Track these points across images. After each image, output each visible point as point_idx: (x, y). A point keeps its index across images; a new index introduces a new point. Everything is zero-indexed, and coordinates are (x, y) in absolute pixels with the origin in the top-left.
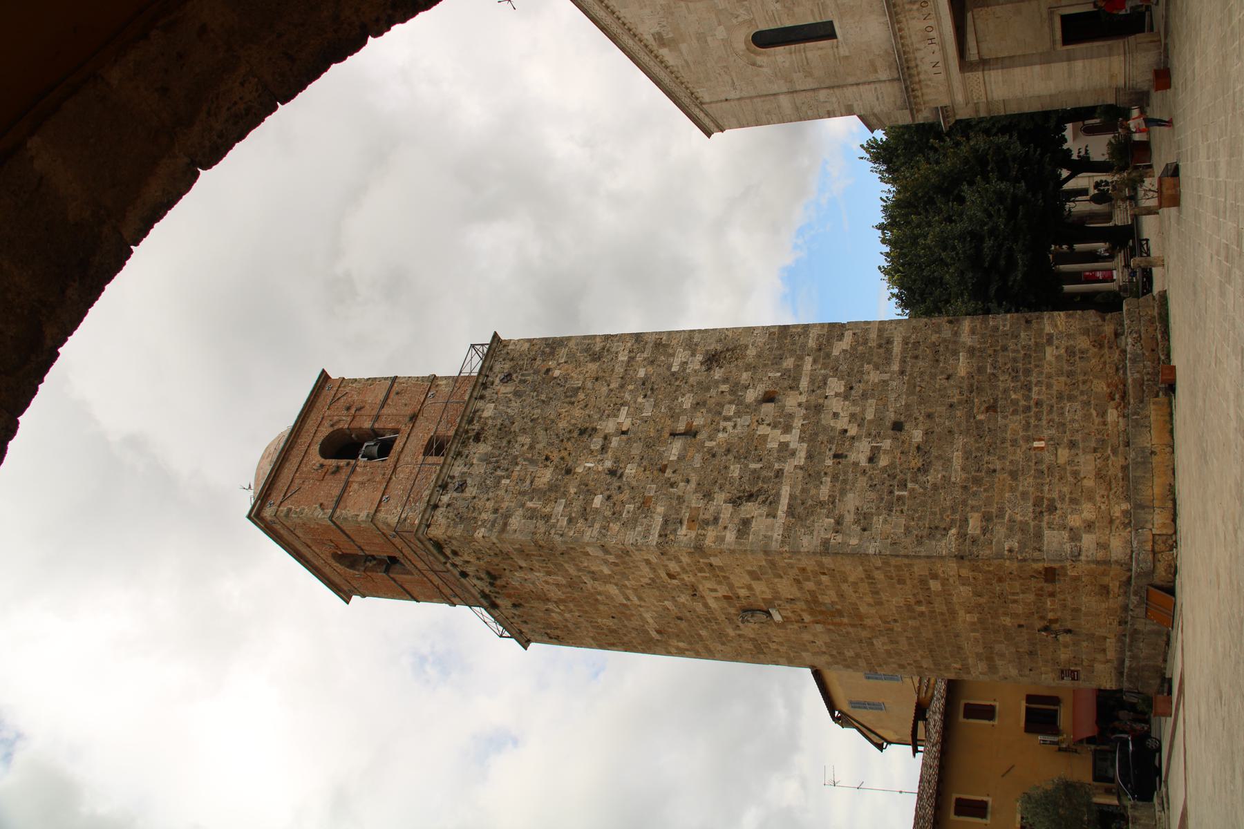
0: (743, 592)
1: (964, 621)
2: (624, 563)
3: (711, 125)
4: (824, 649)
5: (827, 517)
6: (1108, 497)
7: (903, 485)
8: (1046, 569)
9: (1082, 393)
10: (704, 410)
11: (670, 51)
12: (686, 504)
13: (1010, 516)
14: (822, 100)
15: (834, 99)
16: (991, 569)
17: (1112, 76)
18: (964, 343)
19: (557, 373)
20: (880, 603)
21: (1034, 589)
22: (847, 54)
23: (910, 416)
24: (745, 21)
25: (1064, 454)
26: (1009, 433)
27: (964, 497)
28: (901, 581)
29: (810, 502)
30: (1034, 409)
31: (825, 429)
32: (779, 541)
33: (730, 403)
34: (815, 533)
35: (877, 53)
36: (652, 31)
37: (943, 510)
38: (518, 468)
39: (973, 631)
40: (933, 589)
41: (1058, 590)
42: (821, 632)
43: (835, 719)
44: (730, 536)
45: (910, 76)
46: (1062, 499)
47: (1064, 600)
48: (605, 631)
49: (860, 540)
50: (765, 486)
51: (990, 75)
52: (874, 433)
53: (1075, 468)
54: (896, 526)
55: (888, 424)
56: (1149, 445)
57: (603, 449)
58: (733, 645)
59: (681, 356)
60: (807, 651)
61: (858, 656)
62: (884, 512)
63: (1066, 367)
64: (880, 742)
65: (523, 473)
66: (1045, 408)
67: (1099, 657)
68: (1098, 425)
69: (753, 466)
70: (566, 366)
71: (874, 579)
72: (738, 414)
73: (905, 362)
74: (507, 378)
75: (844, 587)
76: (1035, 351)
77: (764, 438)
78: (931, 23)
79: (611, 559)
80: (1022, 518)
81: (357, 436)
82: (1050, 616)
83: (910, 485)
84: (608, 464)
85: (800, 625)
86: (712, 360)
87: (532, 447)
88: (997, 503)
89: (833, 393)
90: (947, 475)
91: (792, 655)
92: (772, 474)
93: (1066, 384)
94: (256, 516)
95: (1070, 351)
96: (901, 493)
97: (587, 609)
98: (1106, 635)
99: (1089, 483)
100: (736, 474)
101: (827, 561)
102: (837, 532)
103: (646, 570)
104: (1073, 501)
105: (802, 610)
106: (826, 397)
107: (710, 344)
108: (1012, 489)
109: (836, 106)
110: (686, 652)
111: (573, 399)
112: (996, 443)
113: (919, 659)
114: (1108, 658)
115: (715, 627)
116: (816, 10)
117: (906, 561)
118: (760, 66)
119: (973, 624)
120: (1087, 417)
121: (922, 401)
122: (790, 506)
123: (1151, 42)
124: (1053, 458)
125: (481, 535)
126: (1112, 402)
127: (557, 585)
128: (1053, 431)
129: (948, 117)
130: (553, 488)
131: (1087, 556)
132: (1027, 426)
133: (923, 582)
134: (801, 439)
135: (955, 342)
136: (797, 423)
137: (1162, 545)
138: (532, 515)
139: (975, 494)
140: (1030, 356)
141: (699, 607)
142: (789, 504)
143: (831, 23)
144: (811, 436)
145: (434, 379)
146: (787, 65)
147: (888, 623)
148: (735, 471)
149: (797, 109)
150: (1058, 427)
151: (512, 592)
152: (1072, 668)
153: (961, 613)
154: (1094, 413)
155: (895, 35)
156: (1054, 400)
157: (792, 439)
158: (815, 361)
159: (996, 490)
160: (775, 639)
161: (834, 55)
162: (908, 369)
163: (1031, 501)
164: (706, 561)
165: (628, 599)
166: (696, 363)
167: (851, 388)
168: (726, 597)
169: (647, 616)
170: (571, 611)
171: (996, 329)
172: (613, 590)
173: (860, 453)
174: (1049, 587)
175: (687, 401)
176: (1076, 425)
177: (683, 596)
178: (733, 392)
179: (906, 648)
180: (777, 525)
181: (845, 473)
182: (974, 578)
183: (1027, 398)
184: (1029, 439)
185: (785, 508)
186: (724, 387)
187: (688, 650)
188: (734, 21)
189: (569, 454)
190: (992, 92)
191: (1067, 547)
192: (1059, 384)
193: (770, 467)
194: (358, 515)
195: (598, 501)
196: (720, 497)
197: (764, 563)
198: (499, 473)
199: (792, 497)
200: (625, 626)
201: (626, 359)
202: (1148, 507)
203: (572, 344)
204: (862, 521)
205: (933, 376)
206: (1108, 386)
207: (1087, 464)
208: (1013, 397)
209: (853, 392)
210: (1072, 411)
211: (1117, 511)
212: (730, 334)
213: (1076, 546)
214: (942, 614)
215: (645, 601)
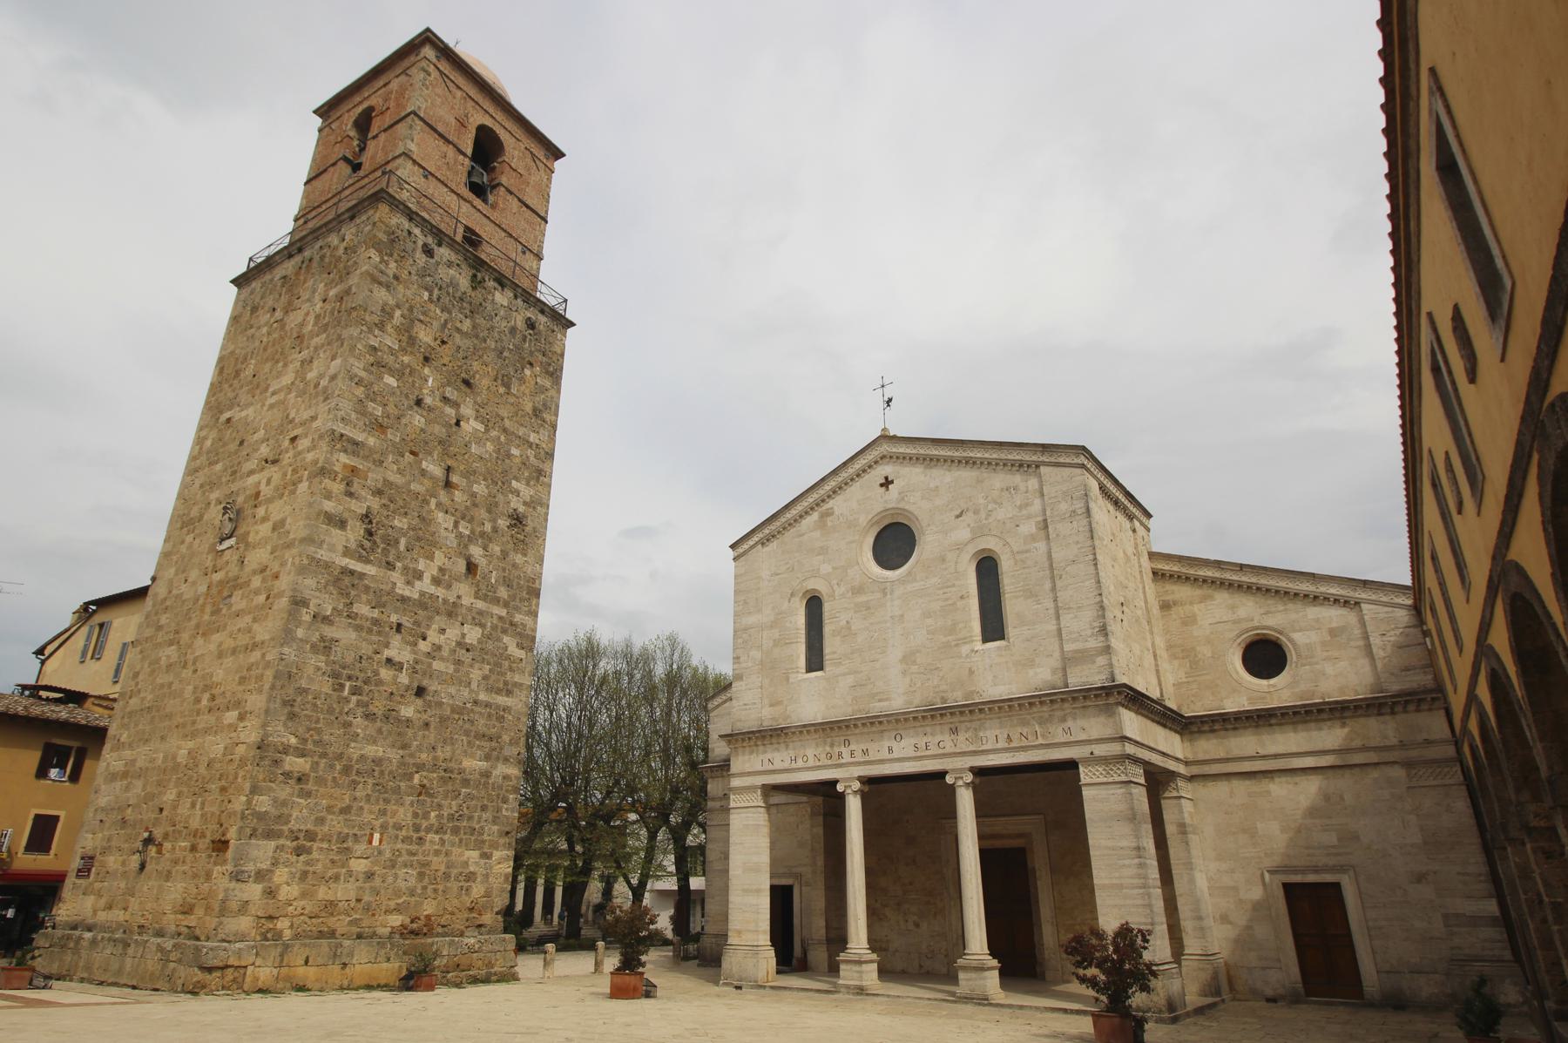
0: (261, 512)
1: (179, 748)
2: (317, 395)
3: (740, 550)
4: (175, 592)
5: (334, 609)
6: (302, 914)
7: (356, 691)
8: (227, 842)
9: (425, 888)
10: (468, 503)
12: (373, 467)
13: (299, 804)
14: (751, 653)
15: (750, 664)
16: (239, 780)
17: (739, 932)
18: (497, 767)
19: (527, 372)
20: (220, 655)
23: (430, 707)
24: (834, 591)
25: (359, 866)
26: (394, 807)
27: (331, 756)
28: (242, 680)
29: (353, 593)
30: (415, 835)
31: (430, 618)
32: (315, 555)
33: (473, 532)
34: (318, 594)
36: (836, 508)
37: (319, 731)
38: (438, 311)
39: (165, 758)
40: (227, 714)
41: (198, 855)
42: (196, 591)
43: (87, 604)
44: (329, 506)
45: (764, 737)
46: (307, 863)
47: (184, 862)
48: (239, 366)
49: (301, 640)
50: (379, 551)
52: (418, 667)
53: (342, 878)
54: (311, 680)
55: (425, 683)
56: (354, 961)
57: (445, 398)
58: (199, 496)
59: (527, 492)
60: (176, 574)
61: (159, 628)
62: (329, 668)
63: (454, 872)
64: (47, 652)
65: (432, 314)
66: (414, 848)
67: (102, 902)
68: (387, 905)
69: (403, 542)
70: (533, 383)
71: (251, 651)
72: (460, 536)
73: (486, 706)
74: (531, 325)
75: (248, 619)
76: (476, 840)
77: (431, 557)
79: (324, 383)
80: (294, 817)
81: (495, 168)
82: (167, 845)
83: (354, 698)
84: (428, 400)
85: (210, 569)
86: (517, 520)
87: (458, 330)
88: (317, 791)
89: (465, 632)
90: (359, 738)
91: (175, 558)
92: (391, 559)
93: (436, 871)
94: (427, 38)
95: (470, 877)
96: (347, 688)
97: (269, 351)
98: (130, 910)
99: (323, 893)
100: (396, 523)
101: (284, 602)
102: (314, 616)
103: (306, 415)
104: (304, 874)
105: (227, 573)
106: (463, 624)
107: (532, 521)
108: (329, 809)
109: (744, 665)
110: (198, 447)
111: (500, 382)
112: (386, 792)
113: (142, 695)
114: (99, 913)
115: (224, 479)
116: (835, 656)
117: (267, 687)
119: (174, 758)
120: (398, 893)
121: (443, 720)
122: (352, 572)
123: (768, 973)
124: (358, 854)
125: (373, 256)
126: (409, 920)
127: (302, 325)
128: (388, 855)
129: (712, 771)
130: (412, 340)
131: (234, 890)
132: (398, 827)
134: (422, 594)
135: (498, 759)
136: (440, 592)
137: (232, 977)
138: (387, 312)
139: (332, 767)
140: (472, 835)
141: (252, 464)
142: (355, 571)
143: (821, 668)
144: (425, 603)
145: (539, 257)
146: (788, 625)
147: (194, 663)
148: (400, 522)
150: (391, 860)
151: (302, 278)
152: (94, 869)
153: (191, 744)
154: (400, 901)
155: (804, 726)
156: (420, 857)
157: (425, 585)
158: (501, 618)
159: (333, 790)
160: (197, 541)
162: (477, 709)
163: (312, 828)
164: (305, 478)
165: (274, 393)
166: (516, 504)
167: (468, 650)
168: (258, 494)
169: (250, 411)
170: (269, 334)
171: (505, 801)
172: (287, 380)
173: (397, 650)
174: (203, 844)
175: (480, 488)
176: (390, 879)
177: (268, 450)
178: (483, 534)
179: (159, 681)
180: (334, 556)
181: (379, 633)
183: (428, 830)
184: (384, 827)
185: (351, 567)
186: (488, 527)
187: (201, 448)
188: (835, 582)
189: (445, 365)
191: (250, 867)
192: (438, 863)
193: (398, 558)
194: (412, 140)
195: (391, 381)
196: (375, 503)
197: (292, 536)
198: (436, 292)
199: (362, 576)
200: (242, 387)
201: (531, 440)
202: (282, 961)
203: (552, 393)
204: (322, 644)
205: (467, 733)
206: (428, 917)
207: (343, 892)
208: (433, 814)
209: (464, 651)
210: (407, 877)
211: (283, 924)
212: (540, 541)
213: (249, 877)
214: (194, 723)
215: (268, 410)
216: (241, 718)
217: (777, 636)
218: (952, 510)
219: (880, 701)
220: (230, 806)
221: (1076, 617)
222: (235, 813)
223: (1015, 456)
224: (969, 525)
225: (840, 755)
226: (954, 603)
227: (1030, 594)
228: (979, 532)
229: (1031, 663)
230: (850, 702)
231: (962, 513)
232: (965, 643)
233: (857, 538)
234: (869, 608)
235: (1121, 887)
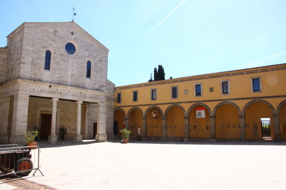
11: (53, 31)
15: (28, 61)
22: (41, 70)
24: (56, 52)
35: (40, 77)
36: (59, 31)
51: (27, 102)
78: (46, 92)
109: (26, 61)
118: (42, 48)
146: (41, 55)
161: (41, 67)
188: (56, 50)
190: (21, 101)
217: (37, 56)
218: (85, 48)
219: (65, 82)
221: (103, 79)
224: (88, 53)
225: (55, 92)
226: (83, 68)
228: (90, 55)
229: (95, 84)
230: (57, 80)
231: (87, 50)
232: (84, 76)
233: (63, 42)
234: (64, 60)
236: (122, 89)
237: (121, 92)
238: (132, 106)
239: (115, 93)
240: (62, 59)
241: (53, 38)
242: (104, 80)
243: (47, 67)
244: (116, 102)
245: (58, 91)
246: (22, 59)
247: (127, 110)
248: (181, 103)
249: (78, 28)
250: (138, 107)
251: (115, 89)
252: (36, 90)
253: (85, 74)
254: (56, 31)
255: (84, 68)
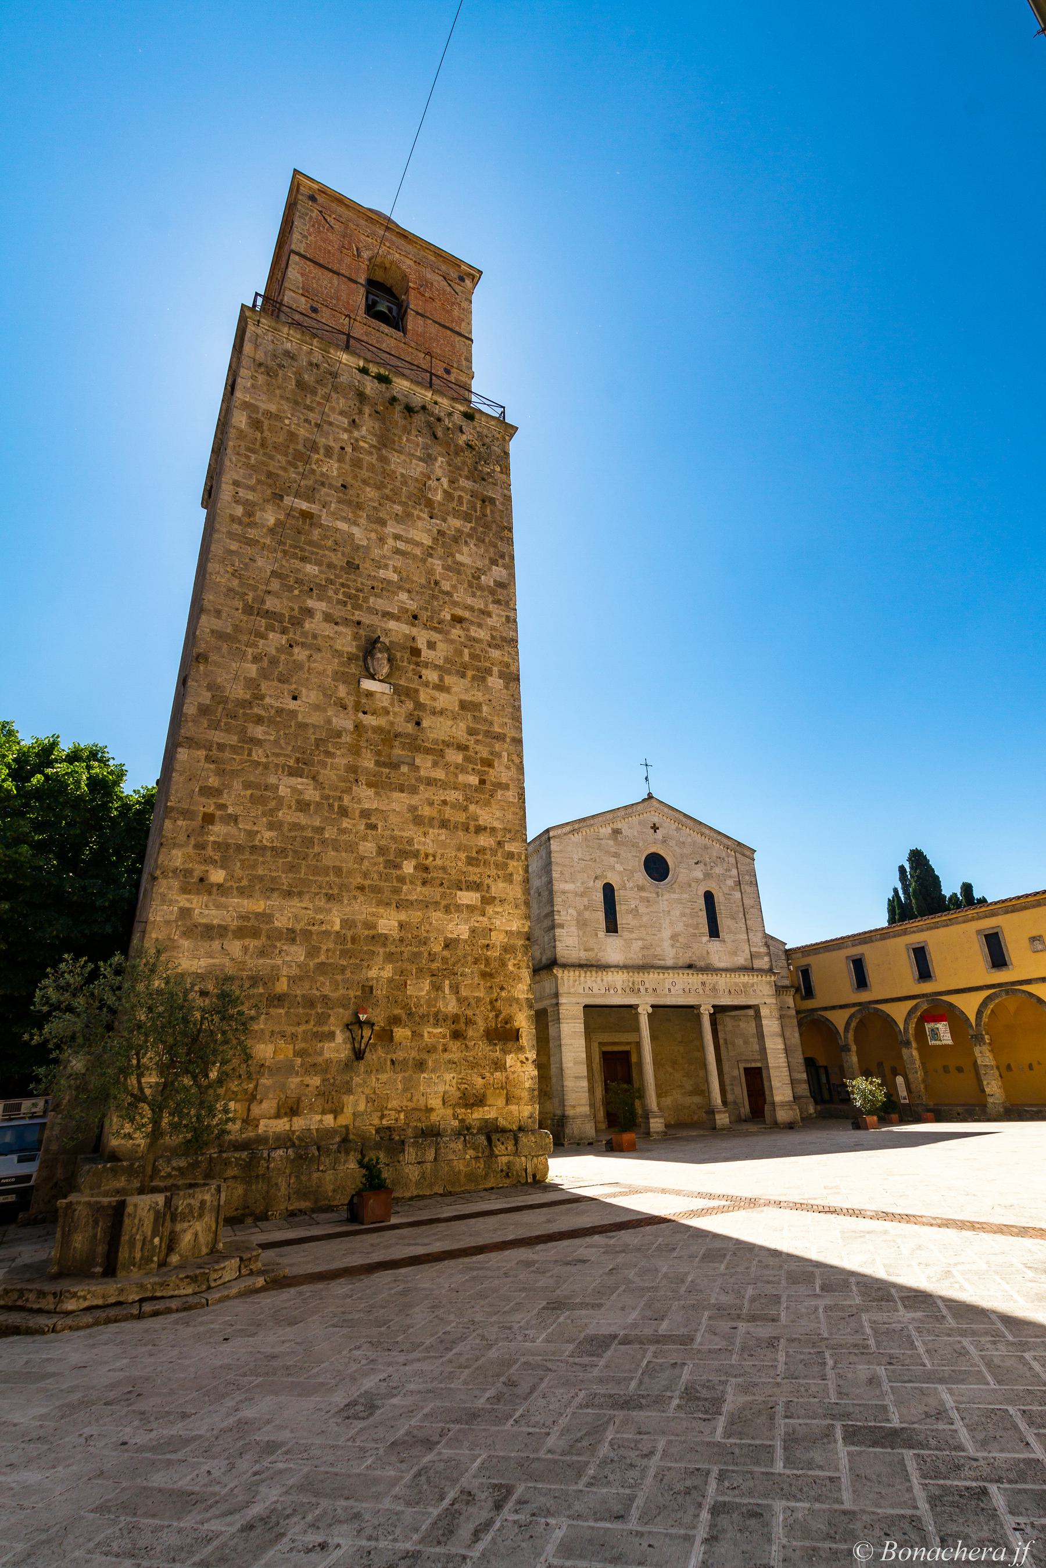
16: (511, 968)
17: (574, 1107)
21: (469, 1013)
28: (471, 861)
39: (347, 923)
40: (459, 893)
78: (620, 991)
117: (518, 878)
119: (370, 926)
133: (476, 886)
149: (564, 893)
182: (488, 945)
216: (487, 901)
217: (586, 903)
220: (504, 994)
222: (517, 1000)
223: (725, 841)
225: (639, 990)
227: (733, 918)
228: (707, 876)
235: (779, 1067)
236: (809, 955)
237: (809, 965)
238: (854, 1005)
239: (791, 967)
240: (642, 899)
241: (613, 850)
242: (757, 939)
243: (612, 927)
244: (798, 996)
245: (647, 985)
246: (556, 917)
247: (839, 1019)
248: (1028, 982)
249: (666, 810)
250: (875, 1009)
251: (789, 953)
252: (596, 991)
253: (705, 929)
254: (617, 832)
255: (700, 913)
